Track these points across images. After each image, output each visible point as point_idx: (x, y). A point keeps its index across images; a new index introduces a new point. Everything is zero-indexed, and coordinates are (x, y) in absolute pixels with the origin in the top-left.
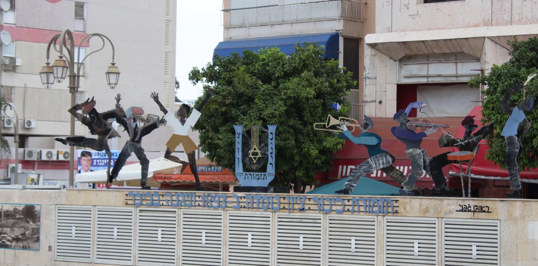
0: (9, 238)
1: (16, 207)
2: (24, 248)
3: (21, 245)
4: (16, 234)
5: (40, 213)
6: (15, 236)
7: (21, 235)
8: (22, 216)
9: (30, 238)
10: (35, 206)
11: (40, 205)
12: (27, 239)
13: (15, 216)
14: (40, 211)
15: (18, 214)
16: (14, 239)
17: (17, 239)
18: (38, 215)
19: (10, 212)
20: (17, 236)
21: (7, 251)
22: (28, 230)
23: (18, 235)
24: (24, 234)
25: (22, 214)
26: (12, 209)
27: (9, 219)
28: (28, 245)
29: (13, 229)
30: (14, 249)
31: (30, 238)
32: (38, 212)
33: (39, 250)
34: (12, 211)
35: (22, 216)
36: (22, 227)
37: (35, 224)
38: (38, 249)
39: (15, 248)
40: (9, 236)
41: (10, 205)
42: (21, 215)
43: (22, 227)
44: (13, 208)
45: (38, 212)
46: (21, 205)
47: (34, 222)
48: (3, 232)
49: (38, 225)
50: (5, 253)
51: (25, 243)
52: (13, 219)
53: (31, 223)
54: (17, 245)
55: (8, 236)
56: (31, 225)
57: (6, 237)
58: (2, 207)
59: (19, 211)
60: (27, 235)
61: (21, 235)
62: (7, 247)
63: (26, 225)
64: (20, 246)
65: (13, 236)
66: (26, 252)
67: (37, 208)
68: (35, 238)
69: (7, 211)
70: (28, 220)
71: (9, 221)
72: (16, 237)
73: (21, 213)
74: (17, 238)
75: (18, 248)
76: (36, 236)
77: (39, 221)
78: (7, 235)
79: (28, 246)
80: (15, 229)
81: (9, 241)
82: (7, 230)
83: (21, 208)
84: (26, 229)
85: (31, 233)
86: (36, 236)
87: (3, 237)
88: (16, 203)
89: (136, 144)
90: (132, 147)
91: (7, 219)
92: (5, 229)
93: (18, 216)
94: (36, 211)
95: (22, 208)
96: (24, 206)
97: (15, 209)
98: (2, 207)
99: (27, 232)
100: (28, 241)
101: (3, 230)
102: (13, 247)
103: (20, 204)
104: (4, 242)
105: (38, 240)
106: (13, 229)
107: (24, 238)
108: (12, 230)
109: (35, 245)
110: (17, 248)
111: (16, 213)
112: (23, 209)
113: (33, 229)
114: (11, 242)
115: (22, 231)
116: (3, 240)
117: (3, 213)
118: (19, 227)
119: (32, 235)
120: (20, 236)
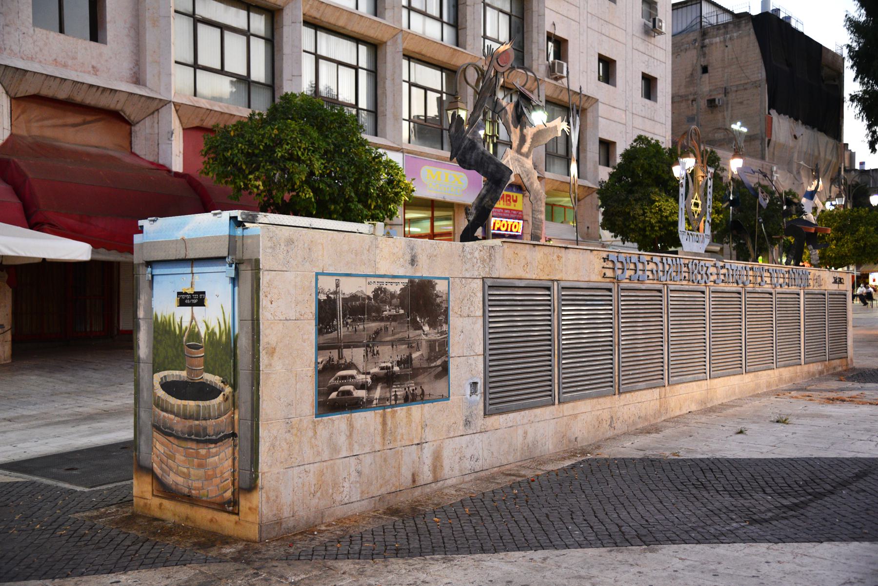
0: (361, 378)
1: (384, 286)
2: (409, 399)
3: (400, 393)
4: (383, 365)
5: (447, 300)
6: (382, 368)
7: (399, 363)
8: (402, 311)
9: (425, 370)
10: (437, 281)
11: (447, 279)
12: (416, 372)
13: (379, 311)
14: (448, 294)
15: (390, 304)
16: (376, 379)
17: (387, 378)
18: (444, 306)
19: (364, 299)
20: (387, 368)
21: (360, 418)
22: (418, 349)
23: (390, 365)
24: (406, 362)
25: (402, 305)
26: (369, 291)
27: (360, 320)
28: (419, 388)
29: (376, 349)
30: (378, 407)
31: (425, 370)
32: (444, 297)
33: (448, 398)
34: (369, 297)
35: (402, 311)
36: (402, 341)
37: (436, 331)
38: (445, 394)
39: (383, 403)
40: (363, 374)
41: (363, 280)
42: (396, 307)
43: (402, 341)
44: (376, 286)
45: (444, 297)
46: (396, 280)
47: (432, 325)
48: (343, 361)
49: (442, 333)
50: (351, 426)
51: (411, 385)
52: (375, 320)
53: (426, 328)
54: (388, 395)
55: (359, 372)
56: (426, 335)
57: (353, 377)
58: (337, 286)
59: (393, 295)
60: (416, 363)
61: (399, 363)
62: (356, 405)
63: (413, 334)
64: (396, 395)
65: (375, 370)
66: (416, 410)
67: (441, 287)
68: (438, 366)
69: (354, 297)
70: (418, 319)
71: (361, 327)
72: (385, 371)
73: (395, 301)
74: (386, 374)
75: (393, 402)
76: (439, 362)
77: (447, 321)
78: (357, 368)
79: (418, 392)
80: (380, 349)
81: (362, 386)
82: (356, 355)
83: (396, 288)
84: (412, 345)
85: (426, 356)
86: (439, 362)
87: (344, 378)
88: (382, 272)
89: (524, 159)
90: (516, 163)
91: (354, 321)
92: (347, 352)
93: (388, 311)
94: (437, 296)
95: (401, 286)
96: (406, 281)
97: (379, 292)
98: (337, 286)
99: (415, 355)
100: (420, 379)
101: (341, 357)
102: (375, 402)
103: (394, 277)
104: (349, 393)
105: (445, 370)
106: (376, 349)
107: (409, 371)
108: (370, 355)
109: (439, 387)
110: (388, 403)
111: (384, 302)
112: (401, 289)
113: (431, 344)
114: (369, 388)
115: (402, 351)
116: (342, 388)
117: (340, 304)
118: (393, 343)
119: (430, 360)
120: (396, 369)
